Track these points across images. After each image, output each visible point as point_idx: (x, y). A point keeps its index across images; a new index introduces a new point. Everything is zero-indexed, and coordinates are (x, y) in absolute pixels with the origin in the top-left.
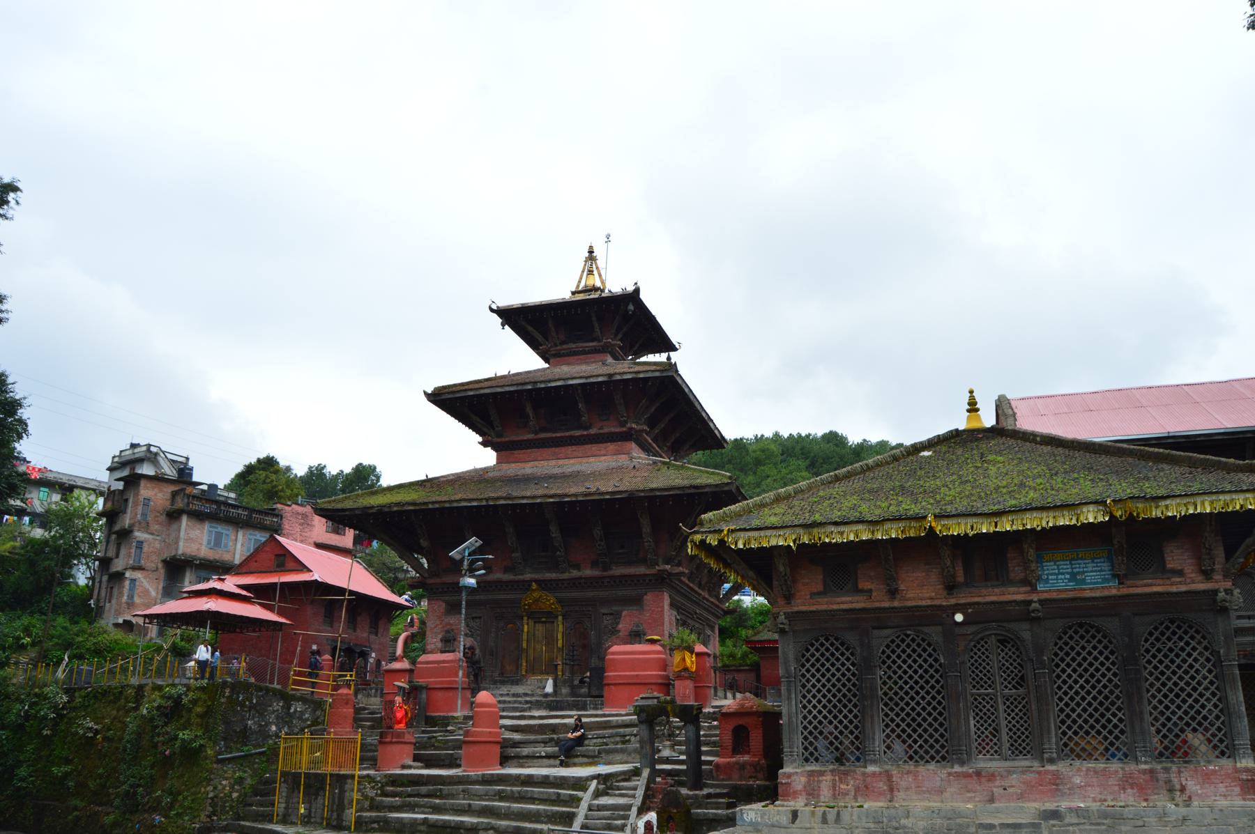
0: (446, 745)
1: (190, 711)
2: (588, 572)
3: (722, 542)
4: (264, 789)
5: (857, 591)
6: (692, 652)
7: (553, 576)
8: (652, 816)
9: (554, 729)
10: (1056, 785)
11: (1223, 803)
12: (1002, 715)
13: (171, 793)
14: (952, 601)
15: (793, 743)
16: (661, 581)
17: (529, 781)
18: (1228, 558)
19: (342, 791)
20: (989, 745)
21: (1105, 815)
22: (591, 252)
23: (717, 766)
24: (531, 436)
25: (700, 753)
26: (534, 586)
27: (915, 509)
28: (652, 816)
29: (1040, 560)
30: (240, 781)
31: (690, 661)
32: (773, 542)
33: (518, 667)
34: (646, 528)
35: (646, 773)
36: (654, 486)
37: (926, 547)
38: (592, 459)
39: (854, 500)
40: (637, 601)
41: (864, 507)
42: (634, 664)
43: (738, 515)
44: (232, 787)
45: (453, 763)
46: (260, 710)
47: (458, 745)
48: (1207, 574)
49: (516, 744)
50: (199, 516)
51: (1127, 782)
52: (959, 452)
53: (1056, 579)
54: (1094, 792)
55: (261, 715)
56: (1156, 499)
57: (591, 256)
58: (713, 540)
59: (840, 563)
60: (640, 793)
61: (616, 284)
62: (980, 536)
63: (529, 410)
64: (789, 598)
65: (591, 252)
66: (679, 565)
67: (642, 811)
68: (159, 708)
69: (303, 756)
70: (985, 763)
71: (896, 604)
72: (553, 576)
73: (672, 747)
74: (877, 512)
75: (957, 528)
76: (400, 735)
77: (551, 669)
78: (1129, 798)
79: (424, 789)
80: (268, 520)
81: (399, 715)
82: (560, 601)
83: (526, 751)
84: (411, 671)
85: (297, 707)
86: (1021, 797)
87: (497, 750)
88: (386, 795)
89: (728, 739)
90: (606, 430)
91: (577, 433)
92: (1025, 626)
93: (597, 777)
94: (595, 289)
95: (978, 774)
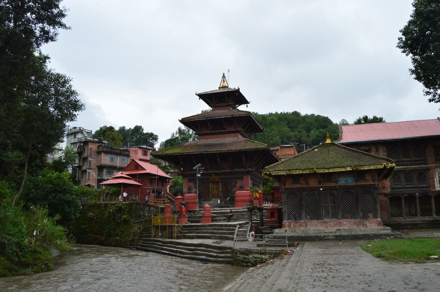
0: (196, 217)
1: (124, 210)
2: (228, 171)
3: (270, 173)
4: (147, 230)
5: (300, 183)
6: (258, 193)
7: (218, 172)
8: (253, 232)
9: (224, 213)
10: (340, 224)
11: (374, 227)
12: (330, 210)
13: (121, 231)
14: (320, 186)
15: (285, 216)
16: (248, 173)
17: (222, 225)
18: (378, 177)
19: (172, 229)
20: (327, 216)
21: (349, 230)
22: (224, 75)
23: (267, 221)
24: (209, 132)
25: (263, 218)
26: (213, 175)
27: (312, 167)
28: (253, 232)
29: (339, 177)
30: (140, 228)
31: (258, 195)
32: (281, 174)
33: (209, 196)
34: (244, 159)
35: (250, 223)
36: (246, 148)
37: (314, 175)
38: (227, 138)
39: (299, 164)
40: (242, 178)
41: (301, 166)
42: (243, 196)
43: (273, 167)
44: (138, 229)
45: (198, 222)
46: (143, 210)
47: (200, 217)
48: (374, 181)
49: (215, 217)
50: (106, 153)
51: (355, 223)
52: (324, 149)
53: (342, 181)
54: (348, 225)
55: (143, 211)
56: (362, 166)
57: (224, 77)
58: (268, 173)
59: (296, 178)
60: (249, 227)
61: (232, 86)
62: (325, 173)
63: (209, 124)
64: (284, 185)
65: (224, 75)
66: (252, 168)
67: (250, 231)
68: (115, 210)
69: (158, 221)
70: (326, 220)
71: (308, 186)
72: (218, 172)
73: (256, 217)
74: (304, 167)
75: (321, 171)
76: (184, 215)
77: (218, 197)
78: (355, 226)
79: (194, 228)
80: (126, 153)
81: (184, 210)
82: (220, 178)
83: (218, 218)
84: (183, 198)
85: (152, 208)
86: (333, 226)
87: (211, 218)
88: (183, 230)
89: (269, 215)
90: (231, 130)
91: (223, 131)
92: (335, 191)
93: (239, 224)
94: (226, 87)
95: (324, 222)
